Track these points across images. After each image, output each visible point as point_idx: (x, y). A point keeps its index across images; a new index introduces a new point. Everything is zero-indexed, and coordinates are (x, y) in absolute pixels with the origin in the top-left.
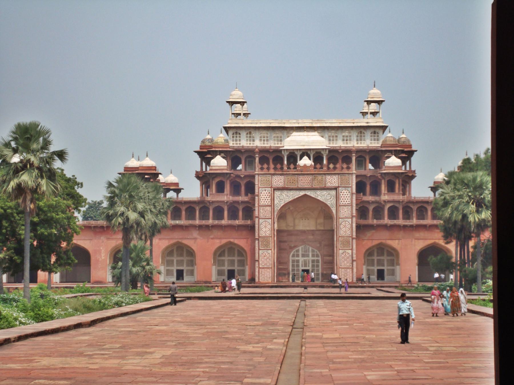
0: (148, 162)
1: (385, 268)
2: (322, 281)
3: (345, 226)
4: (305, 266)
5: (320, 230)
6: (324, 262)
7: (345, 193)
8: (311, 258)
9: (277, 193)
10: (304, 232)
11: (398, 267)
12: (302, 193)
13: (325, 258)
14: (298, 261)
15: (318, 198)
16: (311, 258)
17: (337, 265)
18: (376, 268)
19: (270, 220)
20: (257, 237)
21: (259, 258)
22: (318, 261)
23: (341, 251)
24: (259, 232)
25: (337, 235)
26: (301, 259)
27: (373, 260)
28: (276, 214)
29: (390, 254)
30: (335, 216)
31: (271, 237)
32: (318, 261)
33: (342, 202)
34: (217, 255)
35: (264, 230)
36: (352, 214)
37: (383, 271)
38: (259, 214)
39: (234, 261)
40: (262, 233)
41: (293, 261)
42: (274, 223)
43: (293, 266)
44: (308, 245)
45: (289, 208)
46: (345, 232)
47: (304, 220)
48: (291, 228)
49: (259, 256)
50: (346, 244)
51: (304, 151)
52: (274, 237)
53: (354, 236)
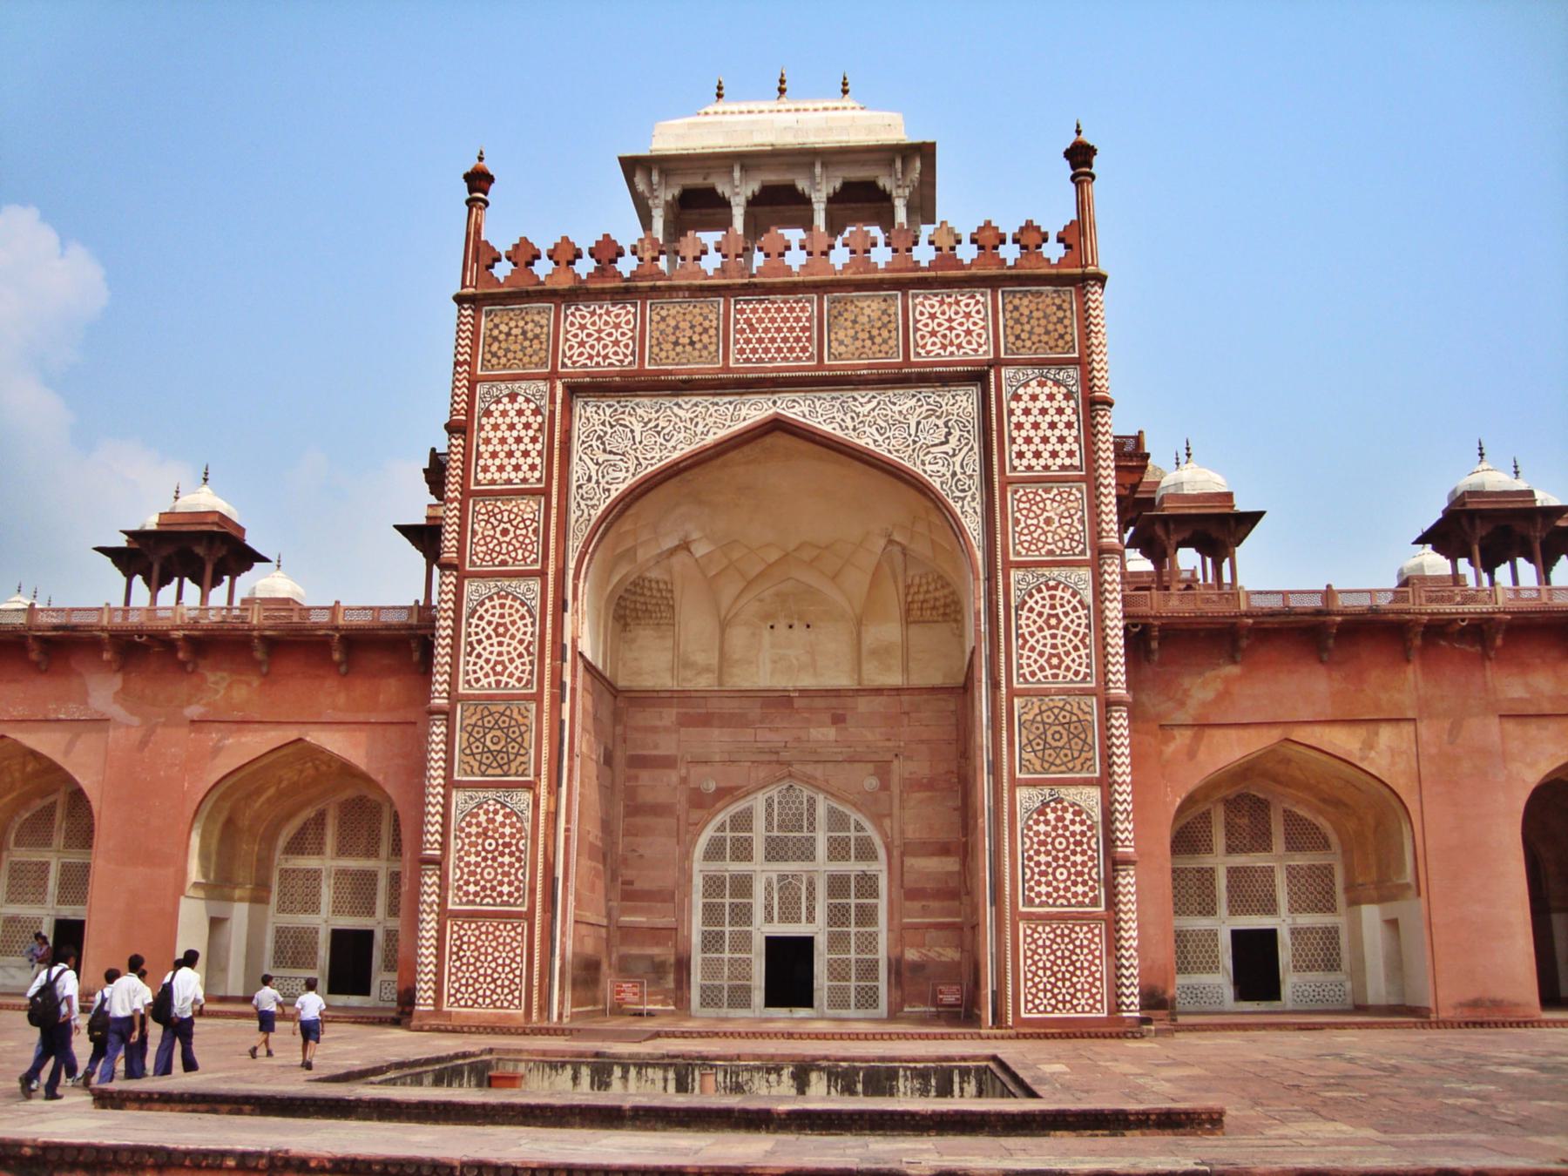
0: (202, 499)
1: (1282, 922)
2: (894, 1015)
3: (1052, 621)
4: (789, 915)
5: (878, 691)
6: (909, 893)
7: (1044, 402)
8: (823, 866)
9: (590, 416)
10: (779, 701)
11: (1371, 915)
12: (754, 410)
13: (910, 861)
14: (743, 885)
15: (862, 442)
16: (823, 866)
17: (997, 898)
18: (1224, 925)
19: (535, 585)
20: (440, 701)
21: (444, 846)
22: (867, 885)
23: (1026, 798)
24: (454, 665)
25: (994, 685)
26: (763, 872)
27: (1207, 875)
28: (575, 545)
29: (1302, 836)
30: (979, 555)
31: (538, 698)
32: (867, 885)
33: (1020, 458)
34: (282, 842)
35: (489, 650)
36: (1097, 534)
37: (1270, 936)
38: (461, 550)
39: (369, 877)
40: (476, 676)
41: (714, 885)
42: (561, 606)
43: (712, 913)
44: (809, 781)
45: (685, 546)
46: (1055, 660)
47: (781, 627)
48: (704, 682)
49: (445, 834)
50: (1069, 744)
51: (773, 178)
52: (558, 699)
53: (1119, 689)
